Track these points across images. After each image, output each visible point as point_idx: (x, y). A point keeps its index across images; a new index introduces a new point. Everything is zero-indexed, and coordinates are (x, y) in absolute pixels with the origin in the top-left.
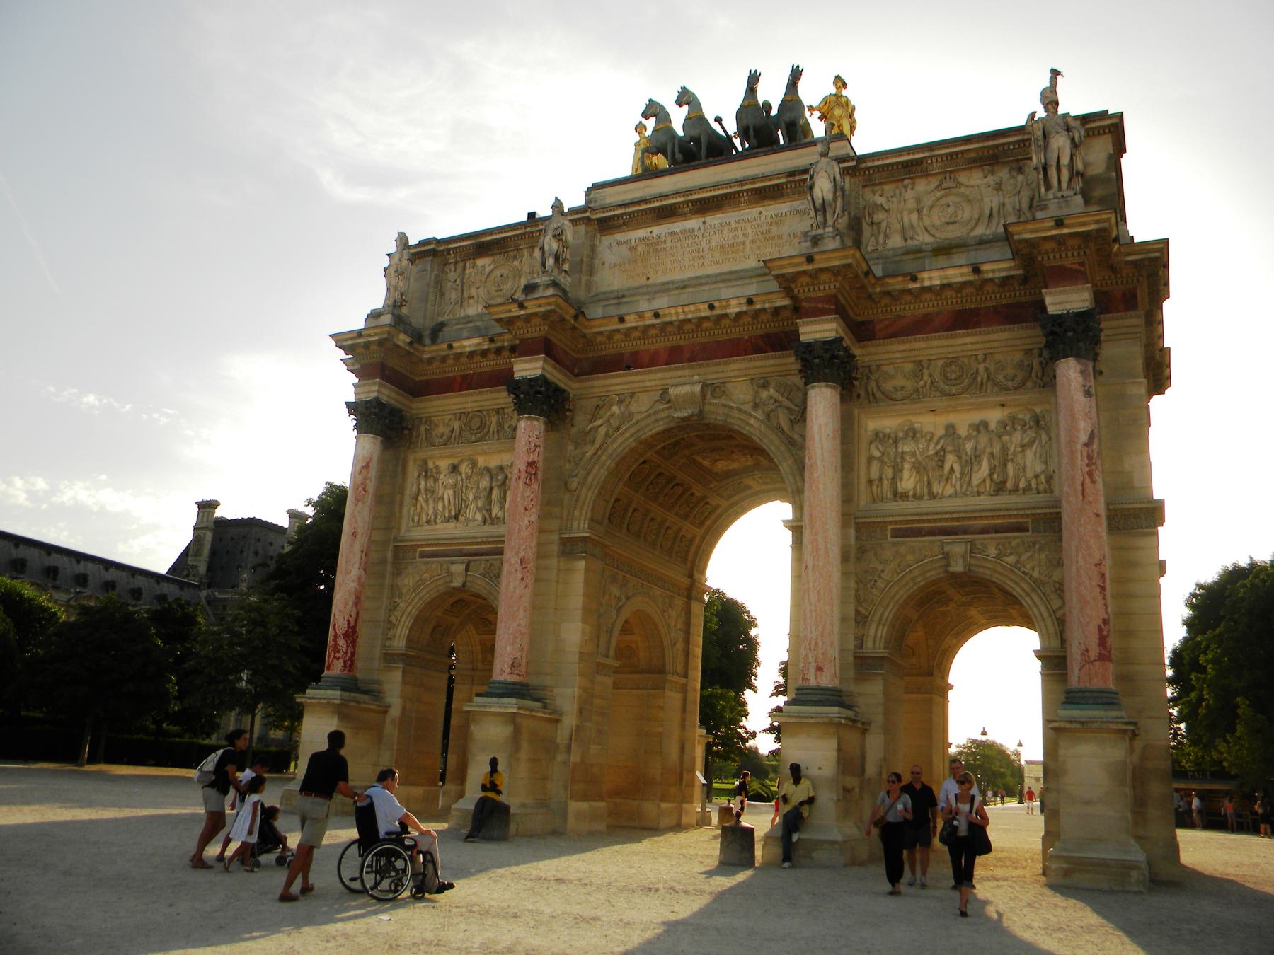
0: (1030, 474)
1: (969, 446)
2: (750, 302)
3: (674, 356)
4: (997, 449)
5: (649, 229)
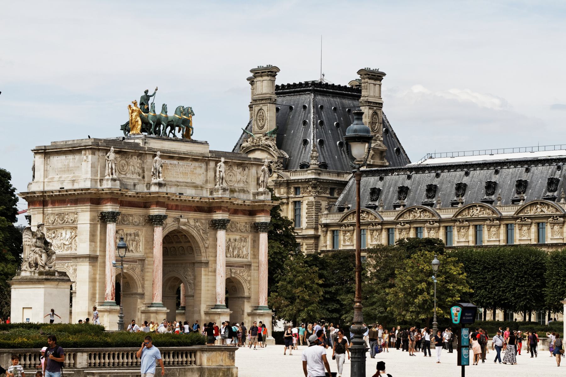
0: (244, 254)
1: (233, 244)
2: (201, 199)
3: (177, 208)
4: (239, 246)
5: (165, 160)
